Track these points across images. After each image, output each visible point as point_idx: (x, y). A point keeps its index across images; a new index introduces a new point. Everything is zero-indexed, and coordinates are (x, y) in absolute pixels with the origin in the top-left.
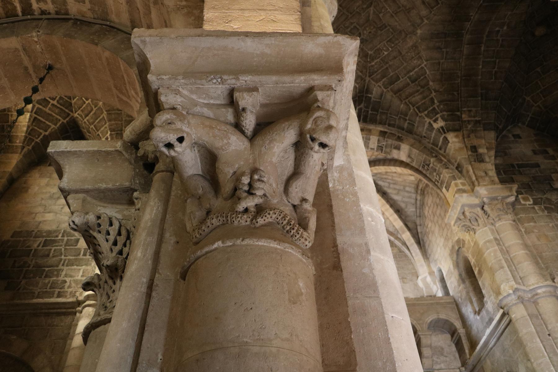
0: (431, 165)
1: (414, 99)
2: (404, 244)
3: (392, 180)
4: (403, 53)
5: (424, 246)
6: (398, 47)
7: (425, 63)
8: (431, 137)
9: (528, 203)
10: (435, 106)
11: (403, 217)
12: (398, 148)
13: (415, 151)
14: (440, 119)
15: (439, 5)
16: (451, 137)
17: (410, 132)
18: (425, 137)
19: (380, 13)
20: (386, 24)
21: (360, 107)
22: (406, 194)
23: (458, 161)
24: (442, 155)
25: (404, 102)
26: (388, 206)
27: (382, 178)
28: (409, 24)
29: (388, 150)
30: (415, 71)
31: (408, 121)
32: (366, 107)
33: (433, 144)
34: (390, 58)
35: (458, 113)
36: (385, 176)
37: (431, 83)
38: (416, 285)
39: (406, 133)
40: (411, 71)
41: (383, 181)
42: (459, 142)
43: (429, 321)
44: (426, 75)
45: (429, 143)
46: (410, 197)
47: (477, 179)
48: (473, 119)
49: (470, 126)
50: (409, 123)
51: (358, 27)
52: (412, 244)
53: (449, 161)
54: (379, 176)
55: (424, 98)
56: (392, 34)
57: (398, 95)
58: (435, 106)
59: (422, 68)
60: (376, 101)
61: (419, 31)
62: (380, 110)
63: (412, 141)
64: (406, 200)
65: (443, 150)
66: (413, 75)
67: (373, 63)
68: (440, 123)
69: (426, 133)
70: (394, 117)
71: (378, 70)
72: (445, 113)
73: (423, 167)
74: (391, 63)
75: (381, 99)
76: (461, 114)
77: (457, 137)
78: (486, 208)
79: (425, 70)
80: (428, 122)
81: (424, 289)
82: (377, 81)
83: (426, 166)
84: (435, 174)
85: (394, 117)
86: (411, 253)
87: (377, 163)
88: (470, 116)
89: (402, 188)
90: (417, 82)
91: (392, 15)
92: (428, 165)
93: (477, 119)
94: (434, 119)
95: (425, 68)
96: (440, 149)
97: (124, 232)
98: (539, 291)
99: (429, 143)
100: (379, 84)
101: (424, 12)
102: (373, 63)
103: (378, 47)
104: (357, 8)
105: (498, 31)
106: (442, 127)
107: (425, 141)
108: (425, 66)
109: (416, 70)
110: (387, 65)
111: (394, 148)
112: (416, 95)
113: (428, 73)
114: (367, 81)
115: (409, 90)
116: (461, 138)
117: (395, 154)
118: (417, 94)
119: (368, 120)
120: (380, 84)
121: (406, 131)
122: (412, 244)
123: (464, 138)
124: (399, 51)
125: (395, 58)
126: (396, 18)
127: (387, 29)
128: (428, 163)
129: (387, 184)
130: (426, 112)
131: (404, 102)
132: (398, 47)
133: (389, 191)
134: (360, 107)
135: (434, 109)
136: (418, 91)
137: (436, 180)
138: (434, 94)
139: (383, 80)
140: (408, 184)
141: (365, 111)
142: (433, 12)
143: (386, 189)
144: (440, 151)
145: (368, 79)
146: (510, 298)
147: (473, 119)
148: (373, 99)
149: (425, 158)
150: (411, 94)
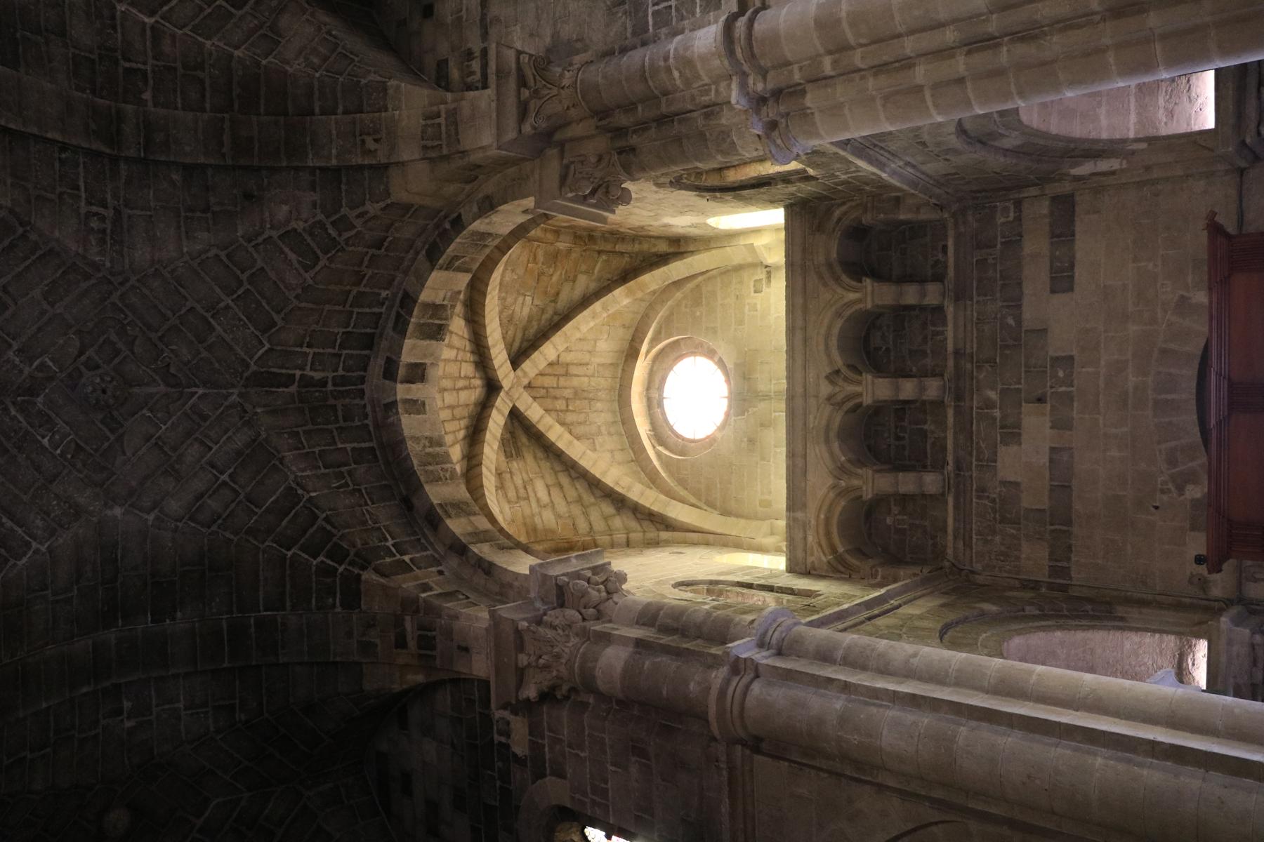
6: (65, 472)
7: (43, 549)
15: (204, 530)
19: (151, 410)
20: (121, 431)
28: (134, 483)
30: (16, 528)
44: (12, 562)
51: (117, 360)
56: (96, 450)
59: (28, 545)
61: (118, 511)
67: (13, 413)
79: (25, 554)
91: (152, 436)
95: (30, 553)
101: (174, 506)
102: (13, 413)
103: (58, 421)
104: (172, 350)
105: (119, 712)
109: (20, 531)
110: (15, 451)
113: (20, 563)
126: (144, 449)
127: (108, 434)
132: (65, 472)
142: (180, 525)
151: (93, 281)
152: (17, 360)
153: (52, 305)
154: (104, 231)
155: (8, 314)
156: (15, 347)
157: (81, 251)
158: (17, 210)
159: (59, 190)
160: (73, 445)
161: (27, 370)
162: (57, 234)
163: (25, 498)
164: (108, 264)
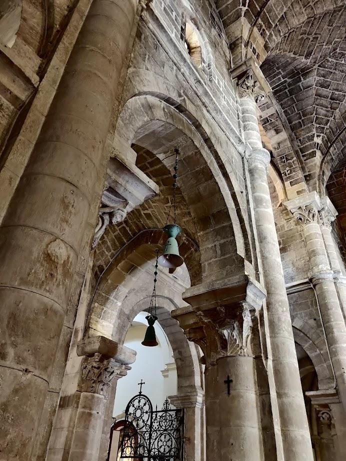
0: (291, 161)
1: (320, 110)
10: (326, 127)
13: (288, 143)
16: (318, 153)
17: (293, 129)
18: (300, 140)
21: (287, 80)
25: (314, 106)
29: (269, 127)
30: (340, 93)
31: (300, 121)
32: (289, 85)
33: (300, 149)
34: (340, 69)
37: (338, 110)
39: (289, 127)
40: (337, 90)
44: (341, 103)
45: (298, 146)
50: (300, 122)
55: (326, 116)
57: (316, 97)
58: (326, 127)
60: (300, 87)
62: (293, 96)
65: (305, 158)
66: (336, 94)
67: (330, 60)
68: (318, 140)
70: (296, 109)
71: (326, 68)
72: (326, 137)
74: (337, 72)
75: (304, 89)
76: (331, 146)
78: (323, 213)
80: (313, 133)
82: (317, 75)
83: (285, 159)
84: (288, 168)
85: (296, 109)
88: (333, 152)
90: (332, 101)
92: (287, 160)
93: (333, 157)
94: (318, 134)
96: (303, 156)
99: (298, 146)
100: (317, 77)
102: (330, 60)
107: (297, 143)
109: (341, 93)
111: (275, 129)
112: (323, 108)
114: (315, 67)
115: (324, 101)
118: (325, 109)
119: (278, 94)
120: (318, 78)
121: (291, 126)
128: (289, 158)
130: (318, 126)
131: (314, 106)
135: (324, 128)
136: (327, 107)
138: (332, 119)
139: (322, 78)
141: (285, 86)
144: (302, 158)
145: (317, 65)
146: (328, 275)
148: (300, 83)
149: (291, 154)
150: (322, 105)
152: (327, 47)
153: (332, 26)
155: (319, 39)
156: (324, 44)
161: (330, 47)
162: (325, 9)
163: (341, 83)
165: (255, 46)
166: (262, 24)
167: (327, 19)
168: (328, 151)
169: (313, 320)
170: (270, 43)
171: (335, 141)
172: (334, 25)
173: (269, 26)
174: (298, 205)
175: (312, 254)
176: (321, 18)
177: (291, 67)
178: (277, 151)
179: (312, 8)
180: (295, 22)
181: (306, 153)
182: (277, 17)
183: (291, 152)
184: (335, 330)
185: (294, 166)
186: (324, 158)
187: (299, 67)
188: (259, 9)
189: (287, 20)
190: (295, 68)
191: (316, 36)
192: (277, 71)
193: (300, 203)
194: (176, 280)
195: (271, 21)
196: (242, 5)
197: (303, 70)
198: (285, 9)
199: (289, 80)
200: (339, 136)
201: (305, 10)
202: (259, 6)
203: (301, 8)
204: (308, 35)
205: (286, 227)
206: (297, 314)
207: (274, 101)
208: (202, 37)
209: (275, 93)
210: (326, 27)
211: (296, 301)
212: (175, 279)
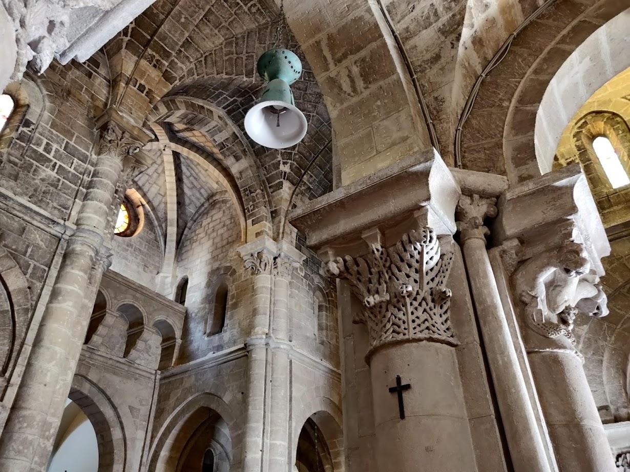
0: (254, 194)
2: (165, 236)
3: (197, 174)
4: (308, 92)
5: (181, 249)
8: (271, 172)
9: (301, 274)
10: (293, 152)
11: (180, 212)
12: (237, 159)
14: (289, 164)
16: (286, 185)
18: (265, 168)
21: (237, 99)
22: (198, 195)
23: (278, 208)
24: (268, 194)
26: (175, 193)
27: (189, 166)
29: (227, 153)
33: (267, 179)
34: (296, 86)
35: (303, 171)
36: (193, 166)
38: (153, 278)
41: (188, 169)
42: (288, 194)
43: (157, 320)
46: (198, 199)
47: (283, 233)
48: (308, 184)
49: (303, 188)
52: (172, 241)
53: (270, 202)
54: (188, 161)
63: (253, 163)
64: (193, 199)
65: (272, 190)
69: (269, 166)
72: (295, 163)
73: (245, 190)
76: (305, 174)
77: (290, 188)
78: (278, 260)
80: (278, 159)
81: (158, 287)
83: (248, 191)
84: (251, 203)
86: (165, 248)
87: (195, 149)
88: (308, 181)
89: (199, 186)
92: (251, 193)
93: (310, 185)
96: (270, 187)
97: (439, 265)
98: (282, 346)
106: (285, 173)
108: (313, 116)
116: (292, 192)
117: (229, 162)
121: (254, 151)
122: (172, 241)
123: (293, 194)
124: (306, 88)
125: (299, 89)
128: (253, 190)
129: (188, 174)
133: (185, 180)
134: (237, 99)
137: (248, 208)
140: (206, 188)
143: (184, 177)
146: (260, 341)
147: (308, 184)
151: (270, 27)
154: (258, 8)
155: (255, 57)
157: (257, 25)
158: (227, 37)
159: (233, 12)
160: (306, 74)
162: (245, 28)
163: (301, 101)
164: (269, 20)
165: (143, 82)
166: (154, 54)
167: (255, 37)
168: (301, 180)
169: (240, 393)
170: (175, 72)
171: (309, 167)
172: (268, 42)
173: (167, 55)
174: (250, 252)
175: (255, 312)
176: (246, 37)
177: (232, 87)
178: (240, 181)
179: (228, 29)
180: (208, 45)
181: (273, 184)
182: (177, 44)
183: (254, 183)
184: (250, 407)
185: (257, 201)
186: (296, 188)
187: (243, 86)
188: (149, 37)
189: (196, 44)
190: (239, 86)
191: (250, 54)
192: (217, 92)
193: (251, 249)
194: (93, 351)
195: (168, 50)
196: (123, 35)
197: (251, 88)
198: (187, 35)
199: (240, 99)
200: (314, 161)
201: (219, 31)
202: (149, 34)
203: (212, 29)
204: (237, 54)
205: (243, 276)
206: (229, 387)
207: (229, 122)
208: (40, 89)
209: (229, 113)
210: (257, 45)
211: (232, 371)
212: (91, 351)
